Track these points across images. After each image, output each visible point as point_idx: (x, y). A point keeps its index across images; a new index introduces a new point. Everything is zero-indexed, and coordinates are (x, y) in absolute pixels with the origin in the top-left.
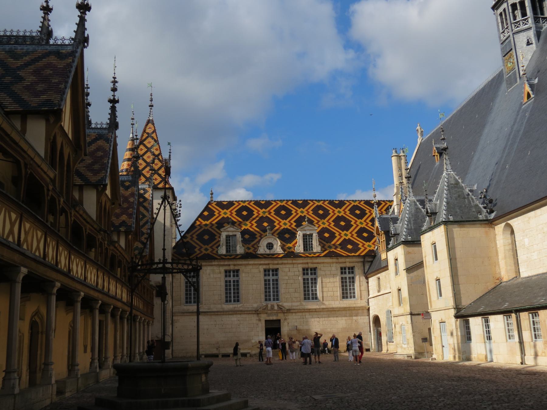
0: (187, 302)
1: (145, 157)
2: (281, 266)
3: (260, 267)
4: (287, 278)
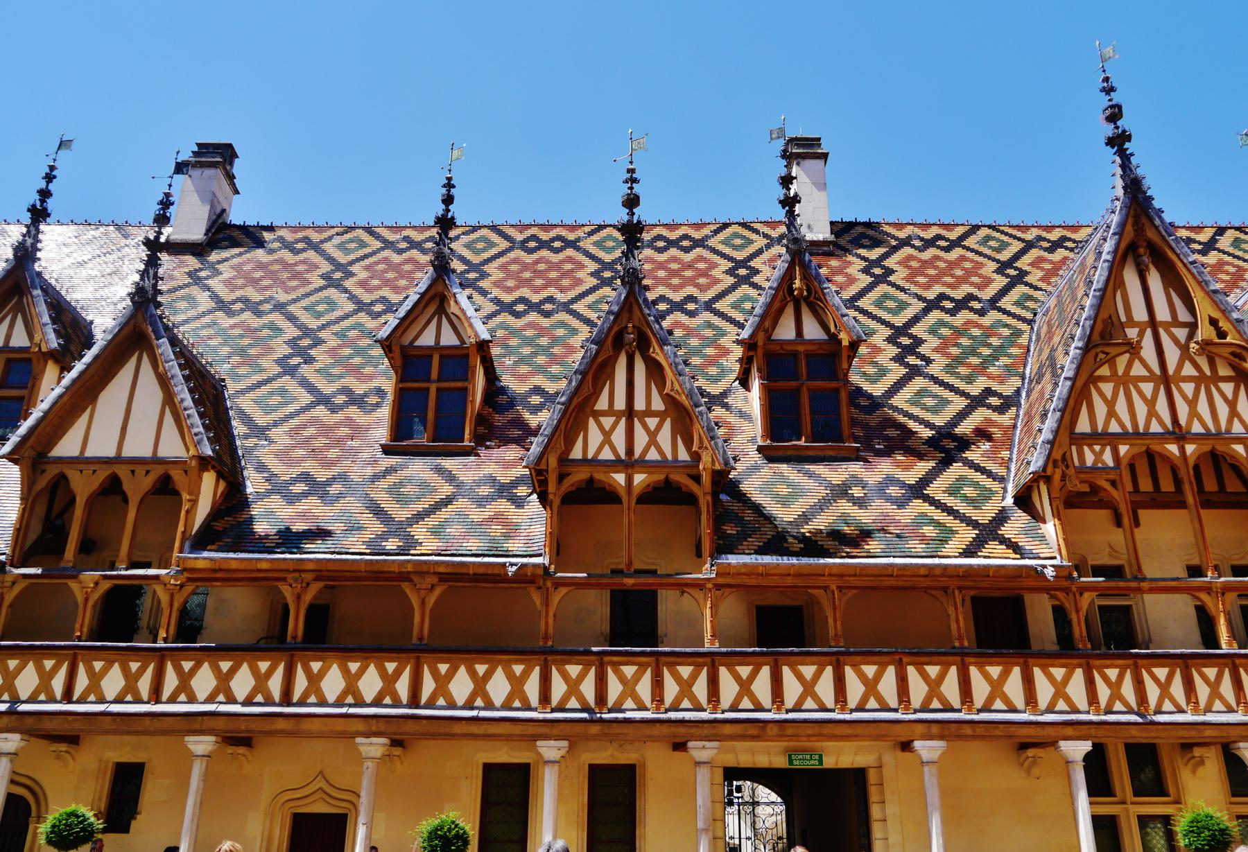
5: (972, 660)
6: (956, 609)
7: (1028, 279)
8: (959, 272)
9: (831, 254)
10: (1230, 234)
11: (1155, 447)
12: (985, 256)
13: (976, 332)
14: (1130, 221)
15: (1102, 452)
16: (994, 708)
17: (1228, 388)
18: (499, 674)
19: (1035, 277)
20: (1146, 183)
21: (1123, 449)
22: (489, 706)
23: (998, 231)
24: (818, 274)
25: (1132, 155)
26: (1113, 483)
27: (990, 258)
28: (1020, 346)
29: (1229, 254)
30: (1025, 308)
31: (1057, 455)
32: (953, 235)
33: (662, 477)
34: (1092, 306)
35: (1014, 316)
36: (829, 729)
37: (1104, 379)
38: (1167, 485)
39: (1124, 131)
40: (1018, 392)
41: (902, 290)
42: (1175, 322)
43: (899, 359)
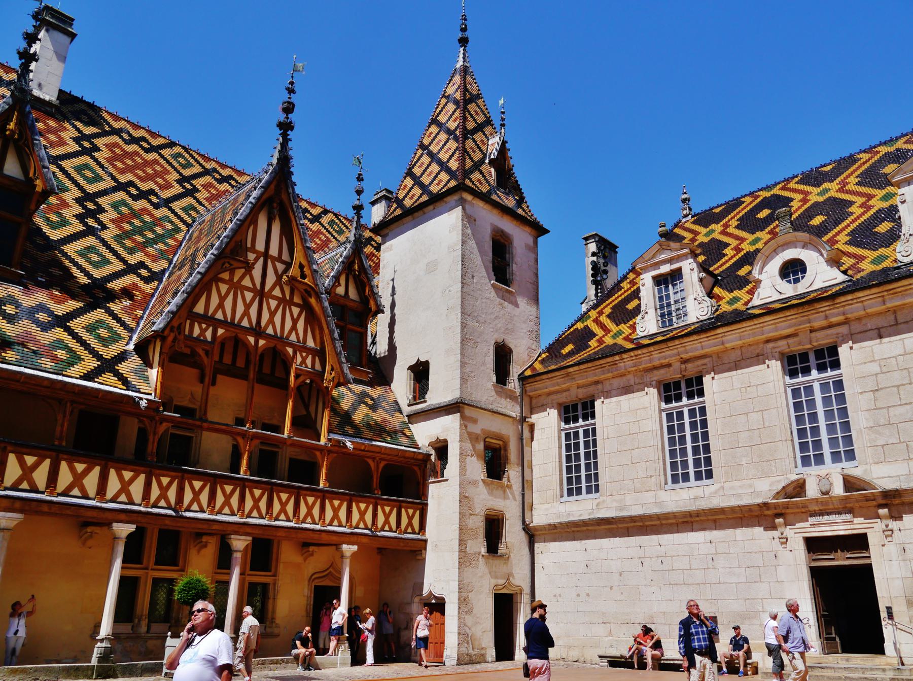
0: (570, 493)
1: (431, 148)
2: (844, 330)
3: (771, 345)
4: (874, 368)
5: (65, 457)
6: (64, 417)
7: (197, 195)
8: (150, 171)
9: (52, 116)
10: (330, 216)
11: (241, 336)
12: (173, 167)
13: (147, 218)
15: (206, 329)
16: (71, 493)
17: (296, 311)
19: (202, 195)
20: (293, 162)
21: (220, 331)
23: (188, 153)
24: (34, 126)
25: (290, 140)
26: (207, 353)
27: (176, 169)
28: (176, 240)
29: (325, 228)
30: (190, 215)
31: (175, 324)
32: (155, 142)
34: (232, 229)
35: (179, 217)
37: (224, 281)
38: (240, 363)
39: (291, 122)
40: (163, 271)
41: (102, 166)
42: (279, 259)
43: (80, 218)
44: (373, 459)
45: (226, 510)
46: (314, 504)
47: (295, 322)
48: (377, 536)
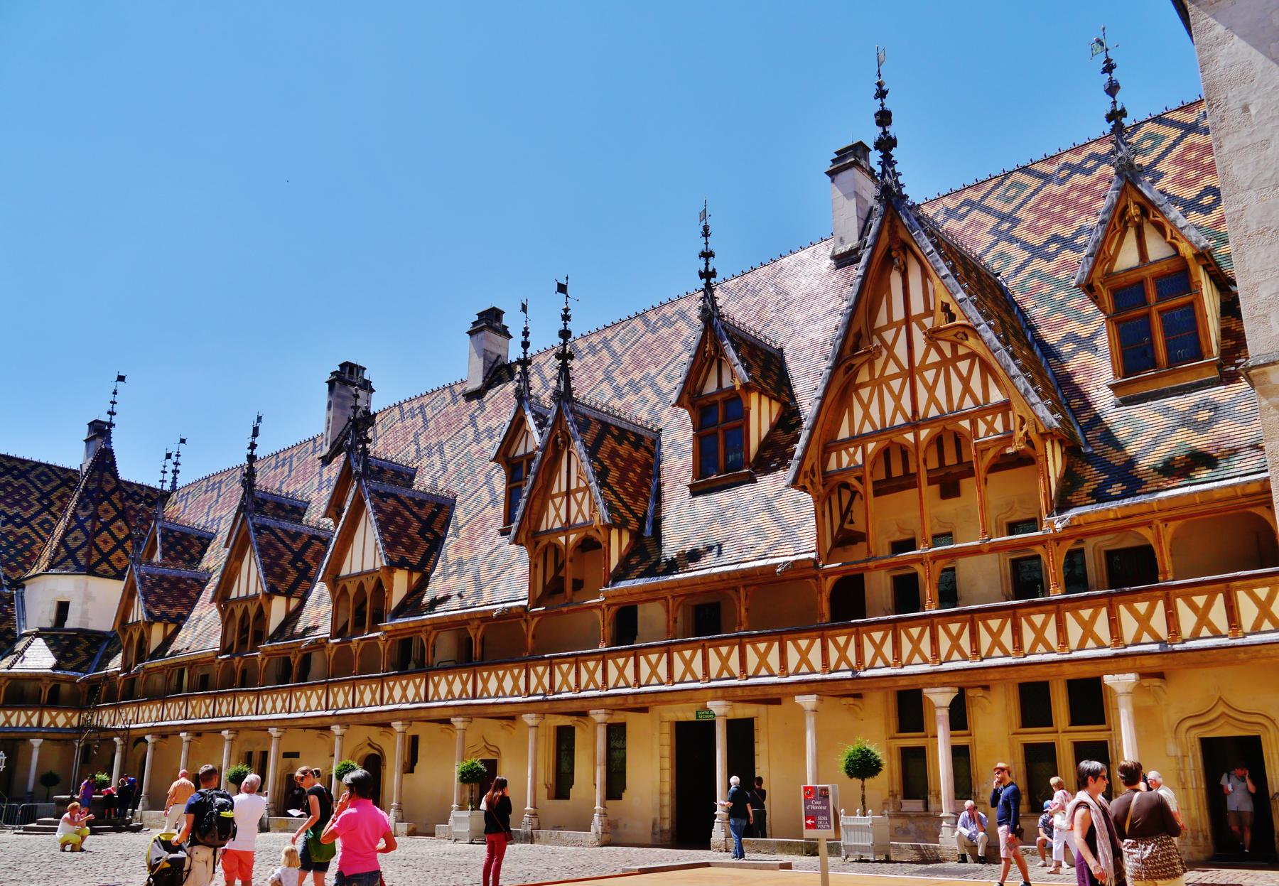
14: (886, 227)
15: (855, 452)
18: (508, 675)
22: (504, 696)
26: (859, 479)
31: (807, 467)
33: (582, 535)
36: (660, 697)
44: (1149, 524)
45: (917, 659)
46: (1045, 624)
47: (966, 381)
48: (1174, 652)
